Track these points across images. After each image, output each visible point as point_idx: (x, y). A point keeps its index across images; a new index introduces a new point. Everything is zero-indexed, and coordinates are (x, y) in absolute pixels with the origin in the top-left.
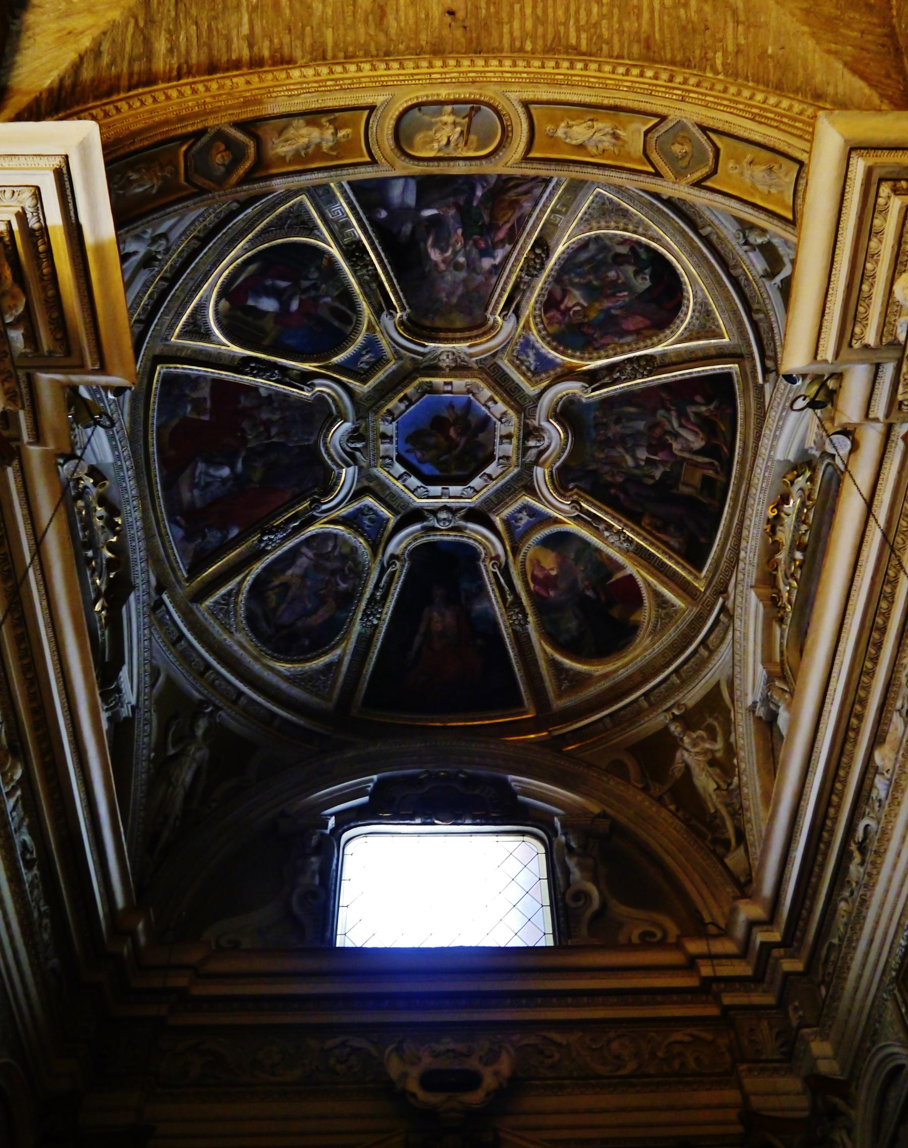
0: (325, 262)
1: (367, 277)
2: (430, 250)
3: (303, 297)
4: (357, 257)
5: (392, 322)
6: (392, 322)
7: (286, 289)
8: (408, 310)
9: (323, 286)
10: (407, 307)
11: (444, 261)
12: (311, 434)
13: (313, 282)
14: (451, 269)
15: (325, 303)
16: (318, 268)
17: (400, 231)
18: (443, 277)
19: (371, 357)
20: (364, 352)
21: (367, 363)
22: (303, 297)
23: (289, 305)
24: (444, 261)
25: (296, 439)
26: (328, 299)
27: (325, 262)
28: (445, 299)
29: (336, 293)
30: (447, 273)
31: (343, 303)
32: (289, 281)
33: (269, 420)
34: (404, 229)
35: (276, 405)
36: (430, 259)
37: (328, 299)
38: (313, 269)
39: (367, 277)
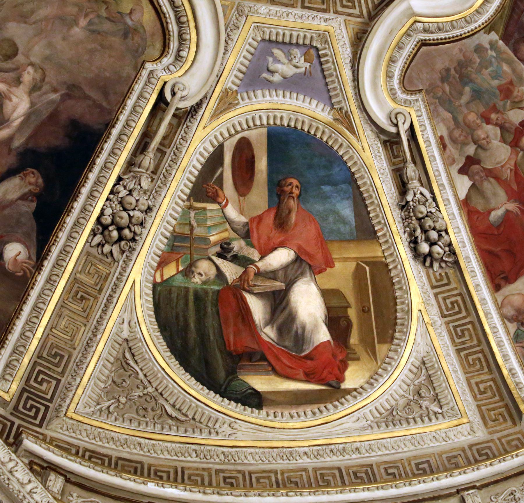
0: (170, 271)
1: (145, 183)
2: (16, 123)
3: (255, 255)
4: (120, 229)
5: (185, 80)
6: (185, 80)
7: (260, 295)
8: (149, 66)
9: (213, 239)
10: (145, 74)
11: (18, 82)
12: (479, 49)
13: (219, 261)
14: (20, 58)
15: (241, 212)
16: (188, 272)
17: (23, 198)
18: (47, 58)
19: (277, 60)
20: (277, 78)
21: (289, 57)
22: (255, 255)
23: (286, 268)
24: (18, 82)
25: (506, 67)
26: (231, 212)
27: (170, 271)
28: (83, 22)
29: (210, 206)
30: (33, 59)
31: (220, 181)
32: (244, 301)
33: (503, 140)
34: (13, 195)
35: (471, 150)
36: (32, 104)
37: (231, 212)
38: (197, 279)
39: (145, 183)
